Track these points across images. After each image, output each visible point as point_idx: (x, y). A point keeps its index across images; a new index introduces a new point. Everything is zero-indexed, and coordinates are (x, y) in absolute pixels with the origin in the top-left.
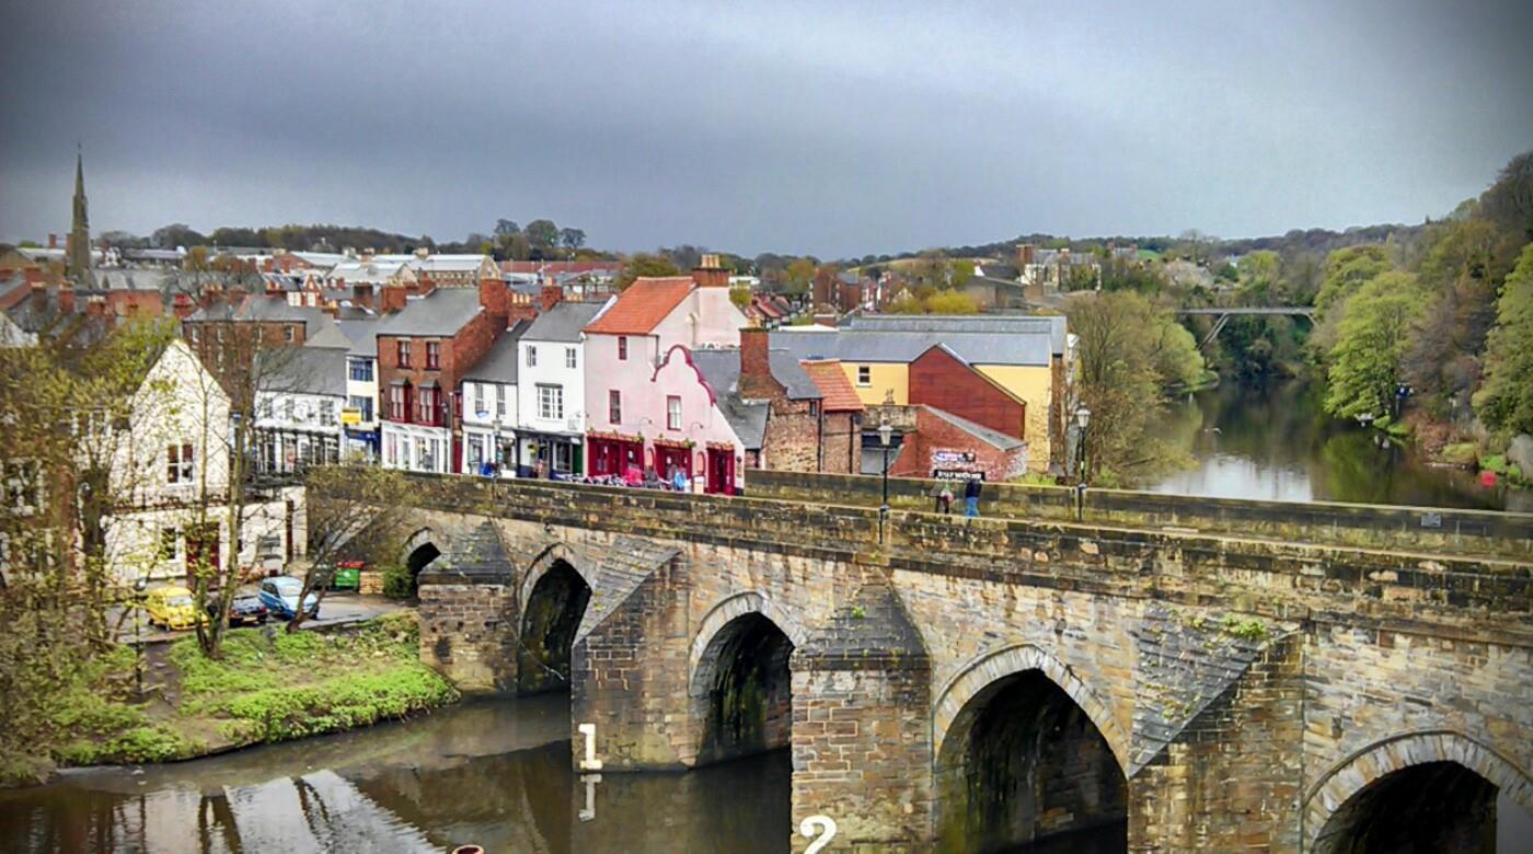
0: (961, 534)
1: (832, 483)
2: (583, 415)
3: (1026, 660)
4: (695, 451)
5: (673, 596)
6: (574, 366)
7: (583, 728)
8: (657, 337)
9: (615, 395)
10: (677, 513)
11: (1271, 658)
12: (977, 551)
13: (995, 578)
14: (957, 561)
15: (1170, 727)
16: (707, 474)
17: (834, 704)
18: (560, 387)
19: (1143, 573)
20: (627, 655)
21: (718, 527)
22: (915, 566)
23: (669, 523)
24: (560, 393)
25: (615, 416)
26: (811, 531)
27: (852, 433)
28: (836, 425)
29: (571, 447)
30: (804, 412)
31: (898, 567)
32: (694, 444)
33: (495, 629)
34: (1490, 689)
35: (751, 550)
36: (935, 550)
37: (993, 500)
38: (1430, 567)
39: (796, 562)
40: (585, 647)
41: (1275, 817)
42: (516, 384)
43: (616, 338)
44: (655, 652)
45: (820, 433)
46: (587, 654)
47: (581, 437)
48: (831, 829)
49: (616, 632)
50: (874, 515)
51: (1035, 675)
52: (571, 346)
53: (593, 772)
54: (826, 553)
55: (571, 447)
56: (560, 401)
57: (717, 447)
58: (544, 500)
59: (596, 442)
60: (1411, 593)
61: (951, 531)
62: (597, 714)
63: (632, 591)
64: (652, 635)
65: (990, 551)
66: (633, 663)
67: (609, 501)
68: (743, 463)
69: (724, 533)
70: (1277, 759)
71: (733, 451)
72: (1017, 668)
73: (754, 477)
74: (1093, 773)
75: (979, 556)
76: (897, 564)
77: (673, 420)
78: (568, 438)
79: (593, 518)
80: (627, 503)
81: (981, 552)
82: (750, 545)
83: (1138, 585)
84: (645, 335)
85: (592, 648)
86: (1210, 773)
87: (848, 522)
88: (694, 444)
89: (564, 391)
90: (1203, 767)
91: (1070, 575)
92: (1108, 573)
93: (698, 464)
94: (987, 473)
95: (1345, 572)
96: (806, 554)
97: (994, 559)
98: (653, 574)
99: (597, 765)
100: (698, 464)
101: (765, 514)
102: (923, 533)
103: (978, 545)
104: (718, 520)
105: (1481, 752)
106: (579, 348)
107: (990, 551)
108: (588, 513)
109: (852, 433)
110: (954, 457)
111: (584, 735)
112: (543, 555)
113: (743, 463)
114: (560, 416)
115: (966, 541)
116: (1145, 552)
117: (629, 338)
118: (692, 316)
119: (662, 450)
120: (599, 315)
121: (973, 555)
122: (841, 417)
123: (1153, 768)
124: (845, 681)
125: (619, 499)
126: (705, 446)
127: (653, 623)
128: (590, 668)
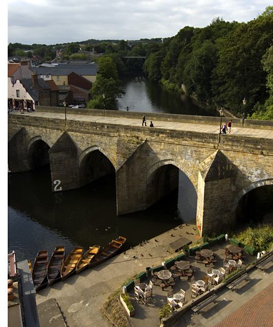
3: (96, 148)
5: (22, 137)
10: (22, 120)
22: (73, 131)
23: (20, 122)
26: (51, 124)
36: (77, 127)
39: (48, 130)
45: (50, 96)
51: (98, 150)
65: (87, 127)
69: (32, 124)
76: (69, 130)
82: (38, 126)
86: (130, 169)
90: (129, 168)
92: (111, 132)
104: (30, 121)
124: (61, 155)
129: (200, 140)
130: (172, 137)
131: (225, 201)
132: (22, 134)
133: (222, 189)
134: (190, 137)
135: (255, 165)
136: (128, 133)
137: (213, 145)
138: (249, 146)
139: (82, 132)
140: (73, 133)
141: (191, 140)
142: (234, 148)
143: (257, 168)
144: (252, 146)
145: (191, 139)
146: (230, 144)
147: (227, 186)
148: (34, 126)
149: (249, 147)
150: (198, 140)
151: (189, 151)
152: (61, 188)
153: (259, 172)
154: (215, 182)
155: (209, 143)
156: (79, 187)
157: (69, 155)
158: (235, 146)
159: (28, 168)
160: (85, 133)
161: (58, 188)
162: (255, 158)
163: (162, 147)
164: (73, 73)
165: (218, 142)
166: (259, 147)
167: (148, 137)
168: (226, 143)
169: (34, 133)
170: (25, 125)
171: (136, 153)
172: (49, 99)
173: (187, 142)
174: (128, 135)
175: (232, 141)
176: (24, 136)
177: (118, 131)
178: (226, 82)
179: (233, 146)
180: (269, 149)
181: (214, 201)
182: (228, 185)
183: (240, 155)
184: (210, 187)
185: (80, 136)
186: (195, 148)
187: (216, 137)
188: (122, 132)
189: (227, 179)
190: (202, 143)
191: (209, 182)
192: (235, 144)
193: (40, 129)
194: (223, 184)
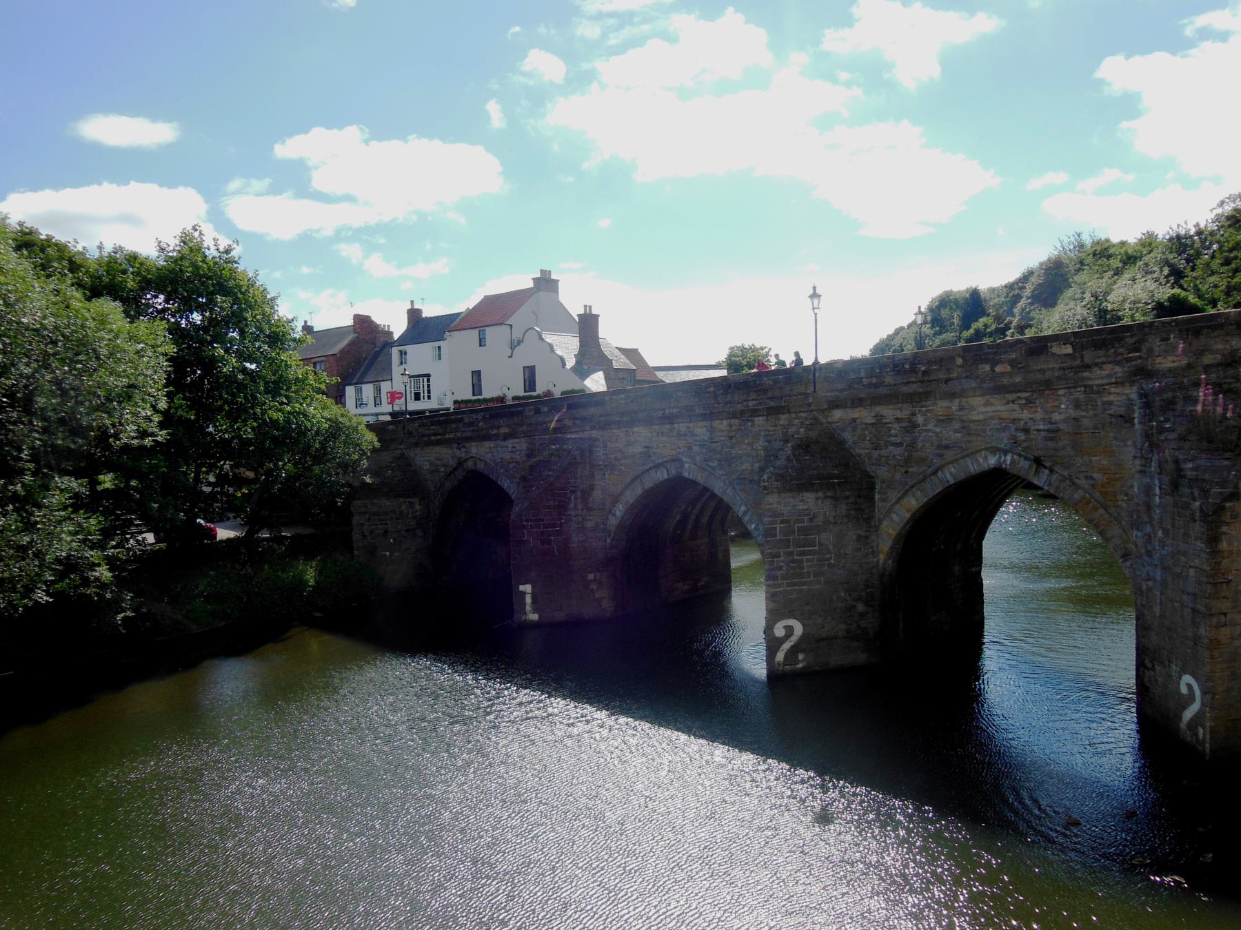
0: (907, 366)
6: (440, 358)
7: (522, 588)
8: (511, 326)
9: (477, 374)
12: (926, 378)
14: (905, 389)
17: (798, 521)
18: (428, 375)
20: (554, 526)
24: (428, 381)
30: (623, 378)
31: (837, 407)
35: (672, 424)
42: (391, 380)
43: (474, 334)
44: (579, 523)
48: (798, 629)
52: (436, 344)
58: (454, 426)
75: (929, 381)
79: (504, 430)
80: (538, 411)
81: (932, 377)
84: (502, 324)
85: (527, 521)
92: (1087, 367)
99: (534, 617)
103: (925, 373)
108: (498, 428)
111: (524, 593)
114: (429, 397)
121: (922, 382)
123: (1228, 504)
127: (576, 499)
140: (855, 413)
152: (801, 657)
185: (898, 420)
193: (682, 427)
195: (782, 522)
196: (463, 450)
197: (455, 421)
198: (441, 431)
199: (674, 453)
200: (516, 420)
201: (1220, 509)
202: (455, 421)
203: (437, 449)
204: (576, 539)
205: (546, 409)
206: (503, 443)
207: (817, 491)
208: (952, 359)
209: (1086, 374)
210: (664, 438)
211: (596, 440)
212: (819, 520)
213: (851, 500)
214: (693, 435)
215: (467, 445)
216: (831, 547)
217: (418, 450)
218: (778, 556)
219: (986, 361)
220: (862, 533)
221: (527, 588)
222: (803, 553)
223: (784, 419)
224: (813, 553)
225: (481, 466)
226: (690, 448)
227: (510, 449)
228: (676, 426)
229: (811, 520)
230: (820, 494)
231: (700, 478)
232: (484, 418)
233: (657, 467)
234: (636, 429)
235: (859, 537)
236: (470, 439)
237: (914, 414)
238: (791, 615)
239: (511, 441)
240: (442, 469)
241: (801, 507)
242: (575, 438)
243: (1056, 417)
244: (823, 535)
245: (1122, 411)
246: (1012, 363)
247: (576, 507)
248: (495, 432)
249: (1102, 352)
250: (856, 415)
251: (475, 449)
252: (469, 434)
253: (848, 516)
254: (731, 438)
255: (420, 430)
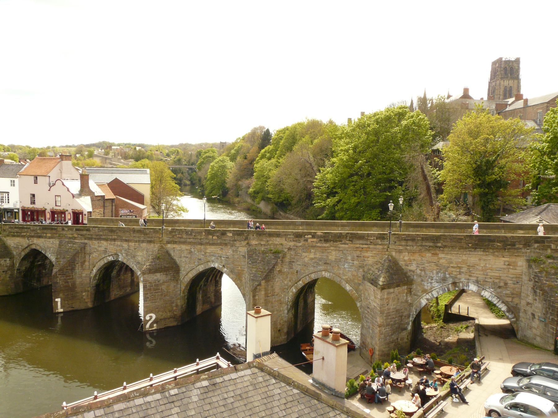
1: (107, 221)
2: (18, 202)
4: (47, 212)
5: (85, 257)
6: (14, 186)
7: (56, 300)
10: (85, 232)
11: (282, 258)
13: (201, 244)
14: (188, 240)
15: (260, 277)
16: (72, 219)
19: (245, 240)
21: (101, 235)
22: (175, 243)
23: (81, 235)
24: (8, 195)
25: (33, 202)
26: (137, 235)
27: (112, 206)
28: (108, 204)
29: (14, 213)
30: (99, 200)
31: (169, 243)
32: (67, 211)
33: (6, 273)
34: (334, 260)
36: (181, 238)
37: (177, 223)
38: (319, 233)
40: (57, 275)
41: (283, 296)
43: (33, 177)
44: (79, 275)
46: (57, 277)
47: (18, 209)
48: (154, 316)
49: (67, 270)
50: (160, 229)
52: (13, 179)
53: (61, 313)
54: (143, 241)
55: (14, 213)
56: (8, 197)
57: (76, 211)
58: (26, 230)
59: (24, 211)
60: (315, 240)
61: (186, 232)
62: (61, 295)
63: (71, 257)
64: (78, 270)
65: (199, 237)
66: (72, 278)
67: (55, 229)
68: (87, 216)
70: (283, 282)
71: (83, 212)
72: (207, 268)
73: (90, 220)
74: (213, 294)
76: (168, 242)
77: (57, 202)
78: (13, 210)
79: (49, 235)
80: (63, 230)
82: (114, 240)
83: (244, 243)
86: (270, 287)
87: (150, 232)
88: (46, 209)
89: (9, 194)
91: (224, 242)
92: (235, 241)
93: (48, 216)
94: (137, 216)
95: (298, 236)
96: (136, 242)
97: (200, 239)
98: (78, 251)
99: (62, 310)
100: (48, 216)
101: (120, 231)
102: (177, 233)
104: (101, 233)
105: (331, 274)
106: (17, 180)
107: (199, 237)
108: (46, 234)
109: (112, 206)
110: (126, 211)
111: (57, 302)
112: (27, 247)
113: (87, 216)
114: (8, 202)
115: (191, 234)
116: (246, 235)
117: (38, 177)
118: (60, 170)
119: (53, 213)
120: (23, 169)
122: (109, 201)
123: (258, 287)
125: (60, 229)
126: (71, 211)
127: (78, 266)
128: (58, 281)
129: (364, 242)
130: (326, 241)
131: (401, 316)
132: (85, 253)
133: (398, 299)
134: (351, 239)
135: (435, 268)
136: (261, 240)
137: (381, 247)
138: (427, 244)
139: (190, 243)
140: (175, 246)
141: (352, 243)
142: (408, 247)
143: (438, 270)
144: (431, 244)
145: (351, 241)
146: (403, 244)
147: (403, 296)
148: (106, 240)
149: (426, 246)
150: (361, 242)
151: (349, 258)
152: (155, 325)
153: (441, 275)
154: (391, 290)
155: (376, 245)
156: (179, 324)
157: (169, 277)
158: (410, 246)
159: (90, 305)
160: (195, 244)
161: (151, 326)
162: (435, 259)
163: (312, 256)
164: (116, 179)
165: (388, 243)
166: (439, 245)
167: (292, 244)
168: (398, 243)
169: (105, 251)
170: (90, 239)
171: (277, 265)
172: (102, 210)
173: (346, 246)
174: (262, 243)
175: (405, 240)
176: (87, 257)
177: (246, 239)
178: (336, 193)
179: (407, 246)
180: (452, 247)
181: (390, 316)
182: (405, 295)
183: (417, 257)
184: (386, 297)
185: (187, 250)
186: (358, 253)
187: (385, 236)
188: (253, 239)
189: (403, 287)
190: (366, 246)
191: (385, 290)
192: (410, 243)
193: (119, 243)
194: (399, 293)
195: (149, 283)
196: (30, 240)
197: (26, 228)
198: (20, 231)
199: (115, 252)
200: (54, 231)
201: (256, 288)
202: (26, 228)
203: (18, 239)
204: (78, 281)
205: (66, 229)
206: (48, 240)
207: (160, 272)
208: (202, 232)
209: (235, 243)
210: (112, 246)
211: (86, 244)
212: (161, 282)
213: (172, 275)
214: (122, 246)
215: (32, 239)
216: (165, 290)
217: (8, 238)
218: (147, 294)
219: (211, 235)
220: (175, 284)
221: (58, 300)
222: (156, 292)
223: (152, 245)
224: (159, 292)
225: (38, 248)
226: (121, 251)
227: (51, 243)
228: (116, 242)
229: (159, 282)
230: (162, 273)
231: (125, 261)
232: (40, 229)
233: (109, 256)
234: (102, 242)
235: (174, 286)
236: (33, 237)
237: (191, 248)
238: (151, 312)
239: (52, 240)
240: (20, 247)
241: (155, 278)
242: (78, 242)
243: (228, 254)
244: (163, 286)
245: (244, 254)
246: (217, 236)
247: (78, 269)
248: (45, 235)
249: (239, 237)
250: (174, 247)
251: (35, 241)
252: (33, 234)
253: (171, 280)
254: (135, 249)
255: (10, 229)
